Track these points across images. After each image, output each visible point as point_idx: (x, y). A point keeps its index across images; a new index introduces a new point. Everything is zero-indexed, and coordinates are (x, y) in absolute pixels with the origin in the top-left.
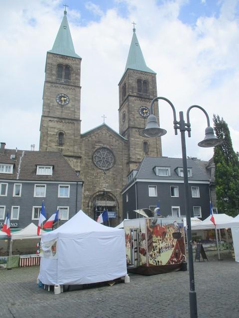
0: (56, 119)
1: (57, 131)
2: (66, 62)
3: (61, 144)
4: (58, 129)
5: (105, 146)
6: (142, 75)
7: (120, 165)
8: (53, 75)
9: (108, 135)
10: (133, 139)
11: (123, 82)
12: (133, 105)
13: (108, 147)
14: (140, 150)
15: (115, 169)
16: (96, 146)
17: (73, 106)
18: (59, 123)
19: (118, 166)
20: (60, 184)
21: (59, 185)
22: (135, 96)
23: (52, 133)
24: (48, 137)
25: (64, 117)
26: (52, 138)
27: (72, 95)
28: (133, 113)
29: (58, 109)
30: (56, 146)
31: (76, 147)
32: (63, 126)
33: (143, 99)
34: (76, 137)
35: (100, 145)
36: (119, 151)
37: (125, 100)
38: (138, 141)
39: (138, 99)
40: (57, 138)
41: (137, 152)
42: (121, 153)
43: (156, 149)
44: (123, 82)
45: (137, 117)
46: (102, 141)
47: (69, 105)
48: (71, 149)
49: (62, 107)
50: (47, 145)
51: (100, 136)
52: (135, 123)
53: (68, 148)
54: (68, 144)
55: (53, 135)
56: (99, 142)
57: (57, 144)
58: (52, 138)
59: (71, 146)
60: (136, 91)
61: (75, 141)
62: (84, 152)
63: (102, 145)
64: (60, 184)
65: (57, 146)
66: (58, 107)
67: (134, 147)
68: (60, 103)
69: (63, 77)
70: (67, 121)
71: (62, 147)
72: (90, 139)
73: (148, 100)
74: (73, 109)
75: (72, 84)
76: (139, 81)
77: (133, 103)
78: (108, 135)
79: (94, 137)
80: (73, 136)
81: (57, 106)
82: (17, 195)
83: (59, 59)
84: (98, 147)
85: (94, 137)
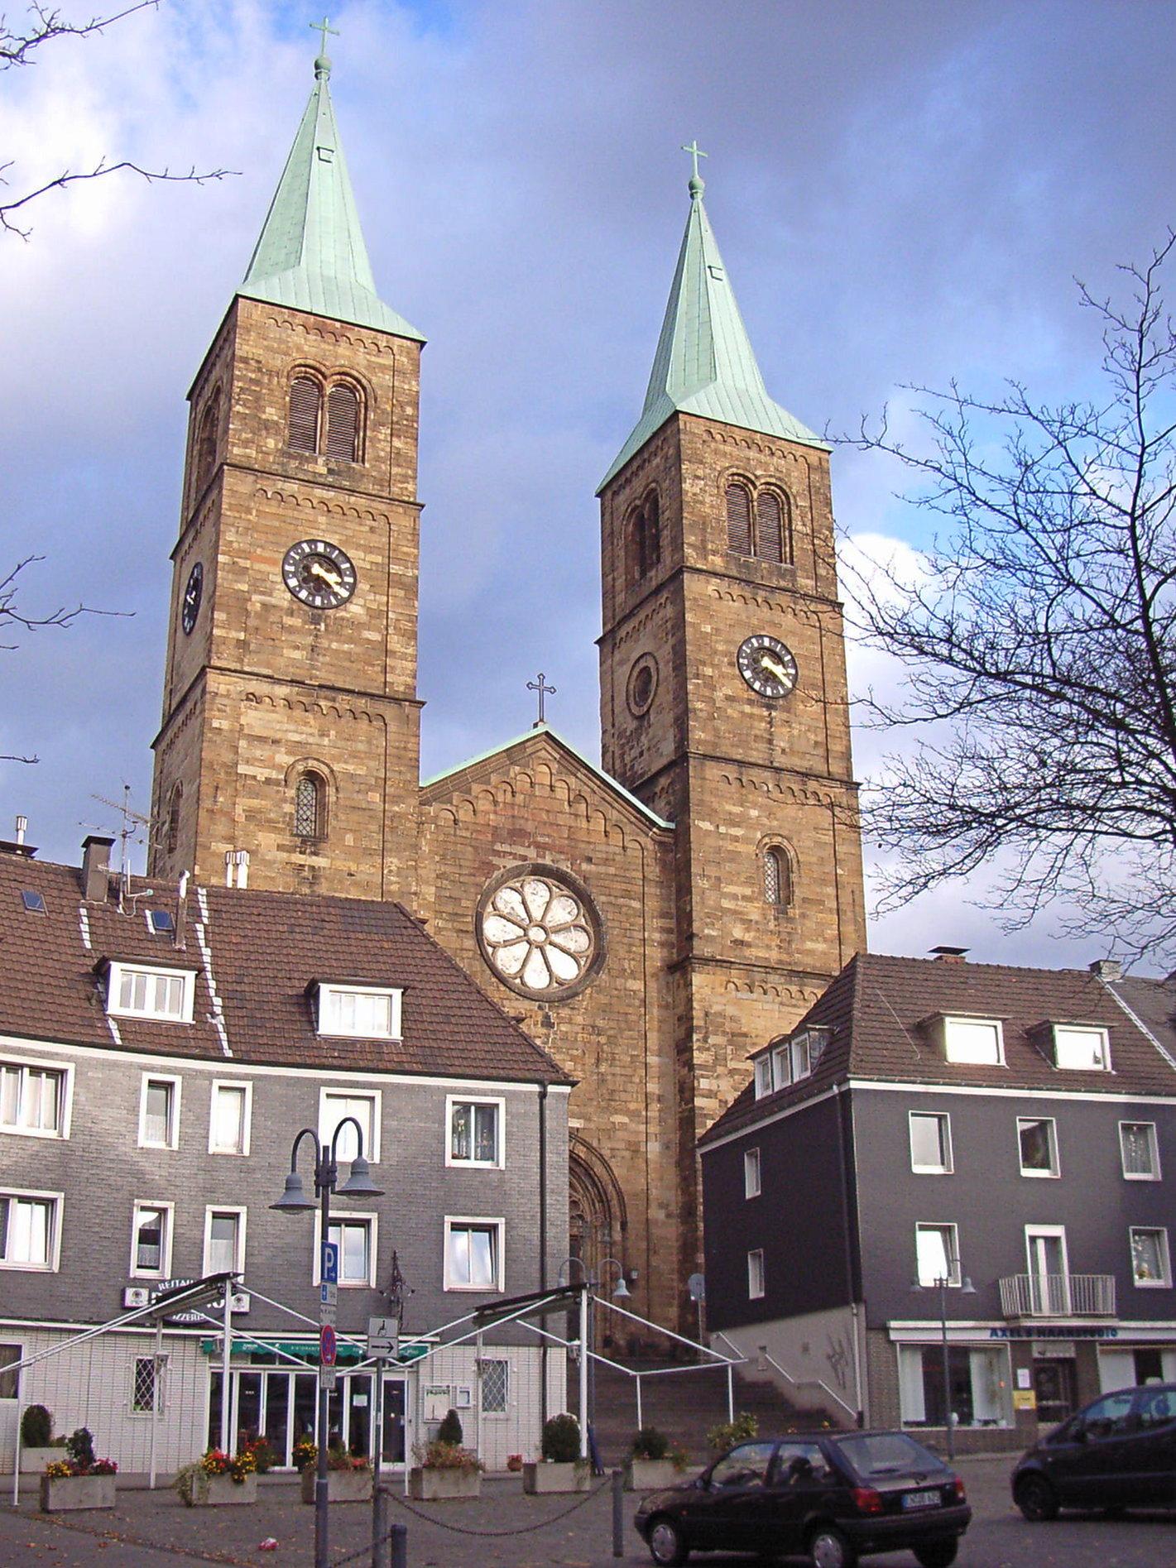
0: (282, 691)
1: (291, 760)
2: (341, 356)
3: (313, 842)
4: (294, 747)
5: (548, 861)
6: (753, 454)
7: (633, 976)
8: (267, 426)
9: (562, 793)
10: (706, 825)
11: (638, 485)
12: (708, 629)
13: (565, 867)
14: (748, 891)
15: (604, 1000)
16: (496, 861)
17: (374, 614)
18: (298, 713)
19: (619, 982)
20: (151, 1069)
21: (217, 1083)
22: (715, 574)
23: (262, 774)
24: (236, 794)
25: (324, 676)
26: (255, 803)
27: (369, 550)
28: (709, 671)
29: (291, 630)
30: (280, 848)
31: (393, 862)
32: (323, 734)
33: (761, 595)
34: (397, 799)
35: (521, 851)
36: (627, 894)
37: (658, 590)
38: (736, 839)
39: (736, 590)
40: (286, 804)
41: (726, 904)
42: (636, 905)
43: (831, 890)
44: (638, 485)
45: (729, 699)
46: (530, 827)
47: (355, 609)
48: (366, 870)
49: (315, 620)
50: (231, 839)
51: (520, 798)
52: (716, 729)
53: (354, 868)
54: (349, 839)
55: (268, 781)
56: (517, 835)
57: (286, 840)
58: (255, 803)
59: (368, 852)
60: (723, 543)
61: (387, 824)
62: (429, 892)
63: (531, 853)
64: (151, 1069)
65: (291, 850)
66: (296, 622)
67: (712, 871)
68: (303, 594)
69: (322, 443)
70: (342, 701)
71: (319, 862)
72: (464, 815)
73: (784, 599)
74: (375, 636)
75: (372, 488)
76: (741, 485)
77: (707, 612)
78: (562, 793)
79: (484, 805)
80: (376, 797)
81: (291, 613)
82: (32, 1125)
83: (298, 337)
84: (511, 863)
85: (484, 805)
